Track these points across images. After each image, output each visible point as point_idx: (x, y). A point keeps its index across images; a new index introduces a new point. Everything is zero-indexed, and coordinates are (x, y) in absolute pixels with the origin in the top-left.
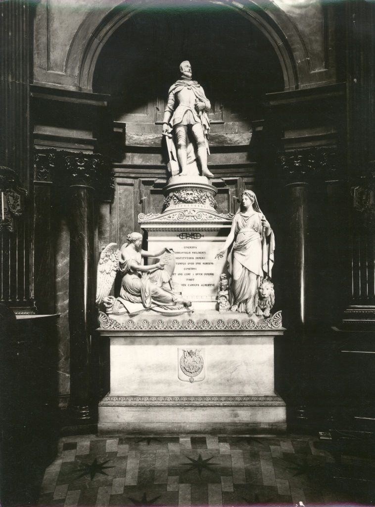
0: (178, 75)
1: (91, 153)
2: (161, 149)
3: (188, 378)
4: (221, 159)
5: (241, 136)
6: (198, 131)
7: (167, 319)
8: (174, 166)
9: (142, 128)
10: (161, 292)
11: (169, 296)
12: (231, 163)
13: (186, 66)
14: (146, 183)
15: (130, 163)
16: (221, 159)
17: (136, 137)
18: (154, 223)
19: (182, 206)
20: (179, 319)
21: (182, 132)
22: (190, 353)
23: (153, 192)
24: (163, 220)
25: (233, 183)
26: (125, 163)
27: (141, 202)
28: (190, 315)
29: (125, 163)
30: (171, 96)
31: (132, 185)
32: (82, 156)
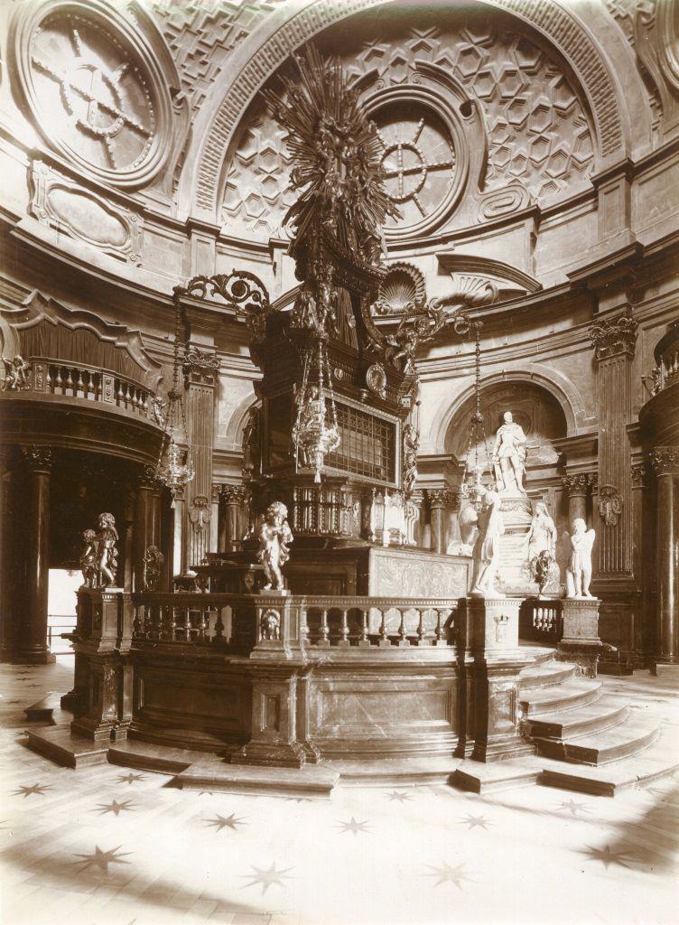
0: (502, 422)
1: (443, 487)
4: (534, 475)
5: (553, 458)
6: (515, 461)
12: (545, 477)
13: (508, 416)
16: (534, 475)
21: (505, 462)
25: (547, 491)
30: (498, 436)
32: (437, 490)
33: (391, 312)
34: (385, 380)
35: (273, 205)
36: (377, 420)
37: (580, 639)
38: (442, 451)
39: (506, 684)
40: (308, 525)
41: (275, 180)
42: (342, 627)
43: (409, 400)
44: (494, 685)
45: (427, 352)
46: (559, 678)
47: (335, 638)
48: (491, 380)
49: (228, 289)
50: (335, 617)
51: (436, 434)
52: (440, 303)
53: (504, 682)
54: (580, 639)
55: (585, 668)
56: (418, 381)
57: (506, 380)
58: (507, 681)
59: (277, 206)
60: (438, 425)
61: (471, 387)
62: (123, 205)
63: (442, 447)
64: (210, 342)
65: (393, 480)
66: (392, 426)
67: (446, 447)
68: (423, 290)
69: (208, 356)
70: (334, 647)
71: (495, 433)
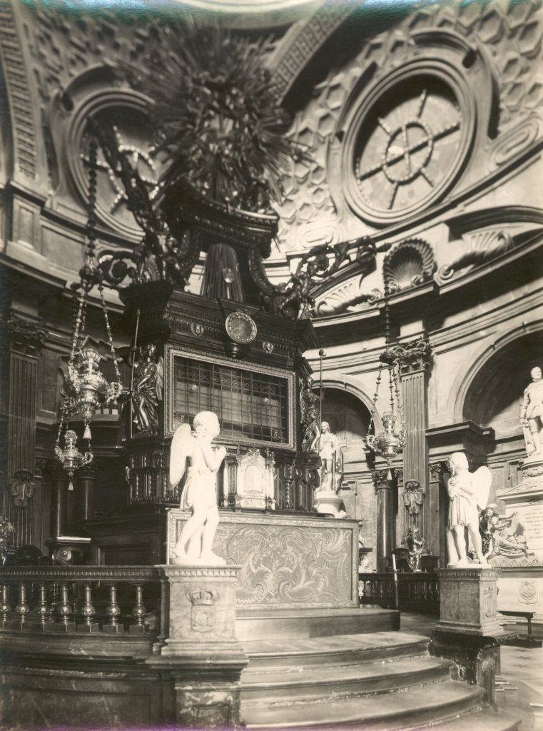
2: (521, 437)
3: (525, 601)
7: (511, 560)
8: (529, 448)
9: (509, 424)
10: (506, 542)
11: (511, 545)
14: (512, 464)
15: (500, 452)
17: (503, 432)
18: (507, 495)
19: (530, 478)
20: (518, 560)
22: (526, 584)
23: (519, 469)
24: (514, 492)
26: (496, 452)
27: (509, 478)
28: (527, 557)
29: (496, 452)
31: (502, 467)
33: (399, 290)
34: (254, 328)
35: (290, 223)
36: (239, 372)
37: (458, 625)
38: (460, 419)
39: (211, 694)
40: (134, 495)
41: (291, 201)
42: (109, 605)
43: (422, 374)
44: (188, 694)
45: (442, 322)
46: (386, 683)
47: (127, 620)
48: (509, 337)
49: (110, 273)
50: (101, 596)
51: (453, 404)
52: (449, 270)
53: (209, 690)
54: (458, 625)
55: (463, 669)
56: (433, 354)
57: (528, 332)
58: (218, 690)
59: (295, 223)
60: (455, 395)
61: (488, 349)
62: (106, 240)
63: (461, 417)
64: (33, 312)
65: (287, 441)
66: (285, 381)
67: (464, 415)
68: (432, 261)
69: (32, 327)
70: (126, 635)
71: (522, 395)
